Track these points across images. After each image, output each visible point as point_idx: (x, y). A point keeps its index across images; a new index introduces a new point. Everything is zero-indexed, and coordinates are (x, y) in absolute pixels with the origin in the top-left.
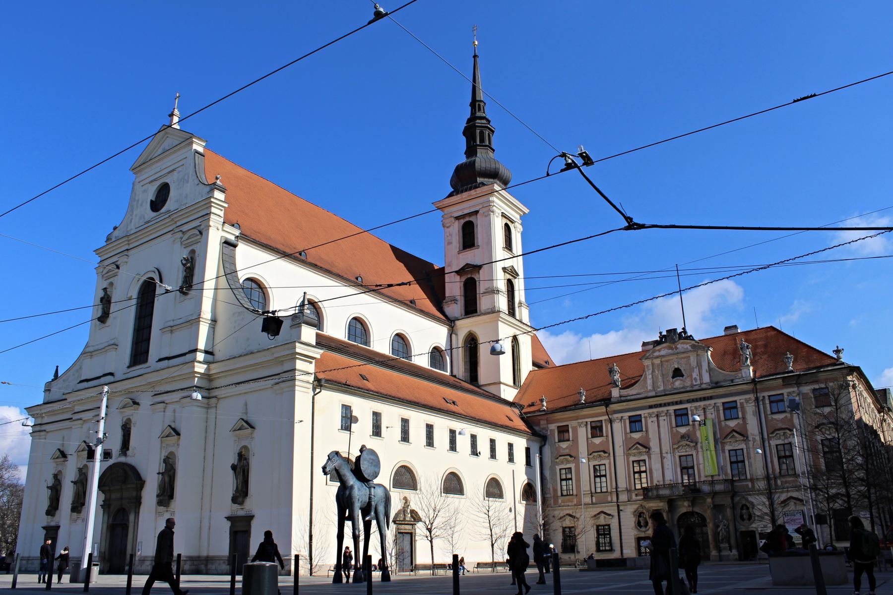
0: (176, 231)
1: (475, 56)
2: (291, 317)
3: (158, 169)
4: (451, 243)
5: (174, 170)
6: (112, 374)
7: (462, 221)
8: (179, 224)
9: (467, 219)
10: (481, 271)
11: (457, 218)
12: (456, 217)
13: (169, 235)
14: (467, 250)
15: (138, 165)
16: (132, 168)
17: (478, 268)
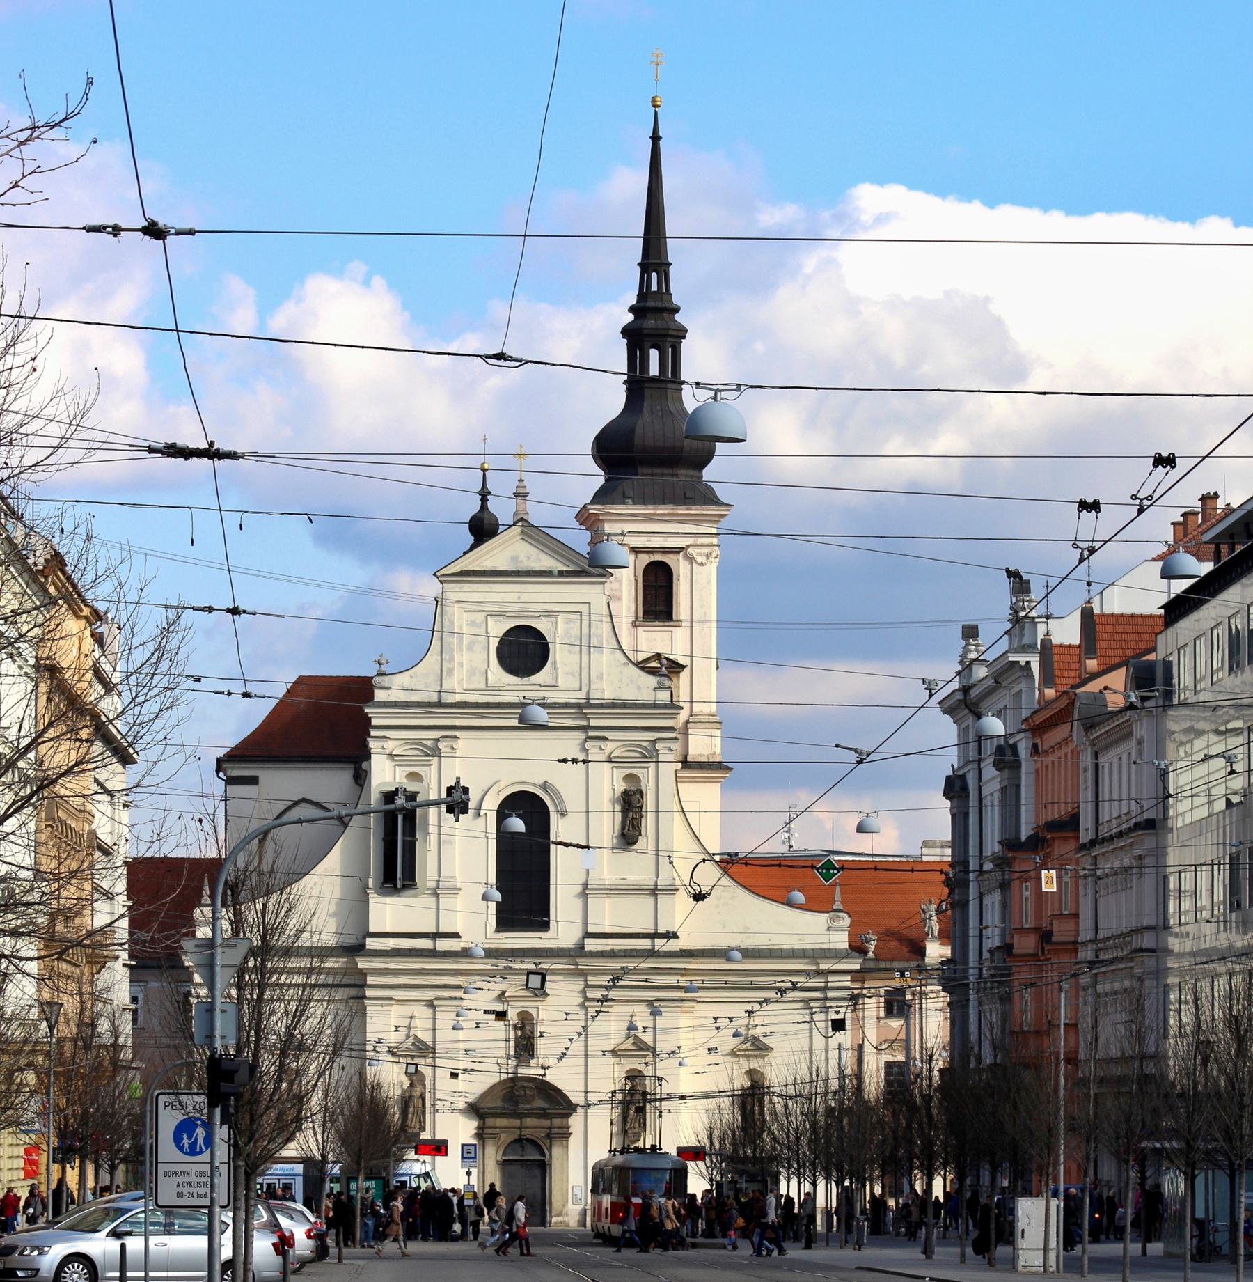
0: (591, 734)
1: (656, 138)
2: (827, 915)
3: (513, 597)
4: (619, 599)
5: (552, 614)
6: (456, 935)
7: (645, 559)
8: (593, 723)
9: (658, 557)
10: (682, 674)
11: (635, 550)
12: (633, 548)
13: (580, 736)
14: (657, 623)
15: (450, 572)
16: (442, 572)
17: (675, 668)
